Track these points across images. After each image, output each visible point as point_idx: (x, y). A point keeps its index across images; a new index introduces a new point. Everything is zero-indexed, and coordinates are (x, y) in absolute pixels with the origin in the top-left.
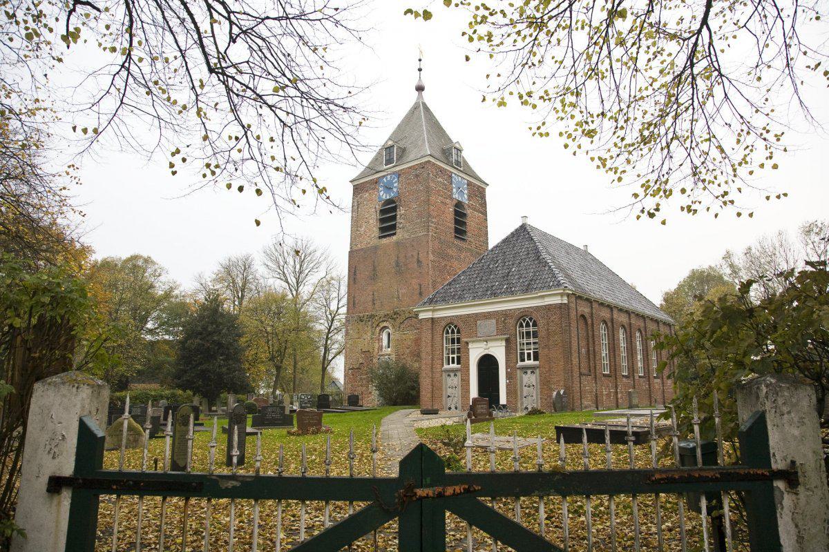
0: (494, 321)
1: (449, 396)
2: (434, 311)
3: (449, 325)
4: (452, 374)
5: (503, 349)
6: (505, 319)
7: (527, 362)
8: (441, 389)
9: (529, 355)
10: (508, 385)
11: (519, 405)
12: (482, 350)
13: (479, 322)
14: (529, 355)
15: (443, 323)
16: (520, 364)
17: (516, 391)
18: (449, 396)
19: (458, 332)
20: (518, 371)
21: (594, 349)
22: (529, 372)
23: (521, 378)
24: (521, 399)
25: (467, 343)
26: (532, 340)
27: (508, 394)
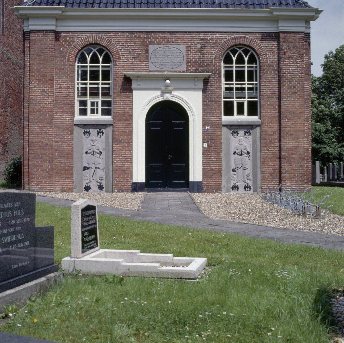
0: (183, 48)
1: (85, 168)
2: (58, 19)
3: (88, 47)
4: (94, 132)
5: (200, 94)
6: (203, 47)
7: (236, 118)
8: (70, 155)
9: (240, 106)
10: (205, 152)
11: (224, 183)
12: (158, 93)
13: (151, 47)
14: (240, 106)
15: (78, 42)
16: (226, 119)
17: (219, 161)
18: (85, 168)
19: (107, 59)
20: (225, 130)
21: (24, 105)
22: (241, 132)
23: (228, 141)
24: (228, 172)
25: (128, 81)
26: (101, 84)
27: (206, 164)
